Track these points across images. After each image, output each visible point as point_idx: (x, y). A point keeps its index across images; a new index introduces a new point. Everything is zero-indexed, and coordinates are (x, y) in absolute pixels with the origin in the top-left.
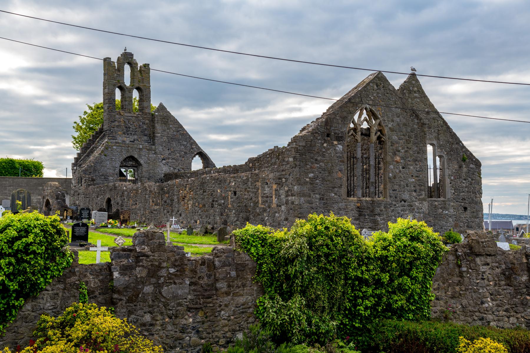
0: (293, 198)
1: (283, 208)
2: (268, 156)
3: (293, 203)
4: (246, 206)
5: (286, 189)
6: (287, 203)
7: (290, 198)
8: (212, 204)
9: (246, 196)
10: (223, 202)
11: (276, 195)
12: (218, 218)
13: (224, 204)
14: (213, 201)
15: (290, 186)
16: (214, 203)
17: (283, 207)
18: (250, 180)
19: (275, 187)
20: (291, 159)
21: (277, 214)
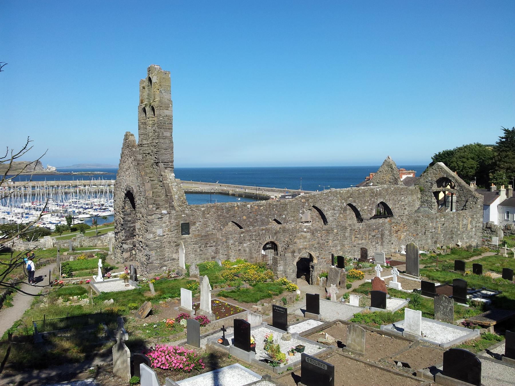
0: (479, 224)
1: (474, 229)
2: (325, 195)
3: (479, 226)
4: (451, 231)
5: (476, 220)
6: (476, 227)
7: (477, 224)
8: (425, 233)
9: (452, 226)
10: (434, 230)
11: (470, 223)
12: (430, 240)
13: (434, 231)
14: (425, 231)
15: (478, 219)
16: (427, 232)
17: (474, 229)
18: (455, 217)
19: (470, 219)
20: (479, 206)
21: (470, 233)
